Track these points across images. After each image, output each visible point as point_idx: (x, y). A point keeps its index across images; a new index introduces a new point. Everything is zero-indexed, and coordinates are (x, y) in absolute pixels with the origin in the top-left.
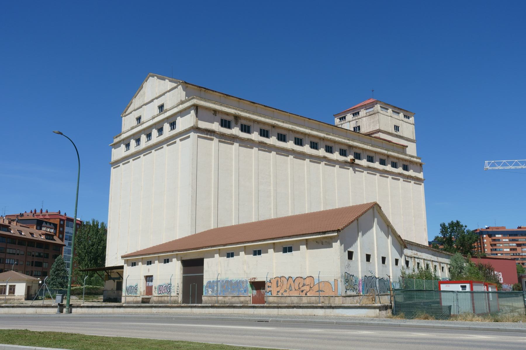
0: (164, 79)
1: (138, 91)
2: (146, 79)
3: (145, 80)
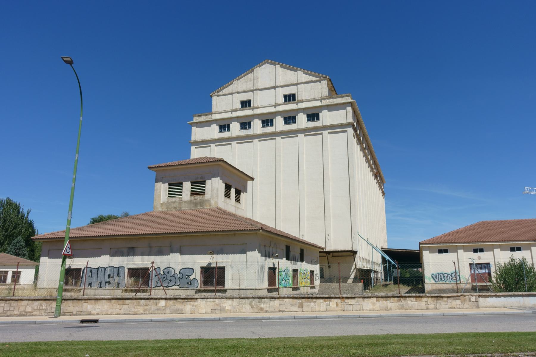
0: (296, 71)
2: (260, 64)
3: (258, 65)
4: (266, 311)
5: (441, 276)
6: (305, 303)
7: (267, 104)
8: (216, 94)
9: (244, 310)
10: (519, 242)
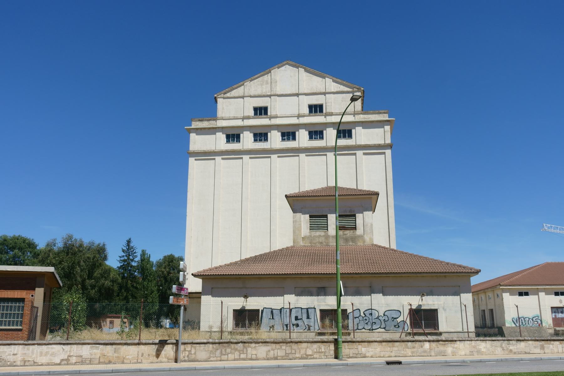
0: (324, 77)
1: (259, 75)
2: (280, 65)
3: (277, 66)
4: (515, 353)
5: (522, 321)
6: (546, 346)
7: (288, 113)
8: (222, 95)
9: (497, 352)
10: (555, 286)
